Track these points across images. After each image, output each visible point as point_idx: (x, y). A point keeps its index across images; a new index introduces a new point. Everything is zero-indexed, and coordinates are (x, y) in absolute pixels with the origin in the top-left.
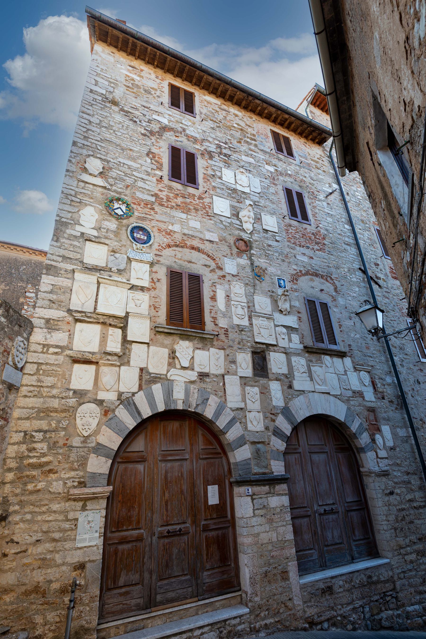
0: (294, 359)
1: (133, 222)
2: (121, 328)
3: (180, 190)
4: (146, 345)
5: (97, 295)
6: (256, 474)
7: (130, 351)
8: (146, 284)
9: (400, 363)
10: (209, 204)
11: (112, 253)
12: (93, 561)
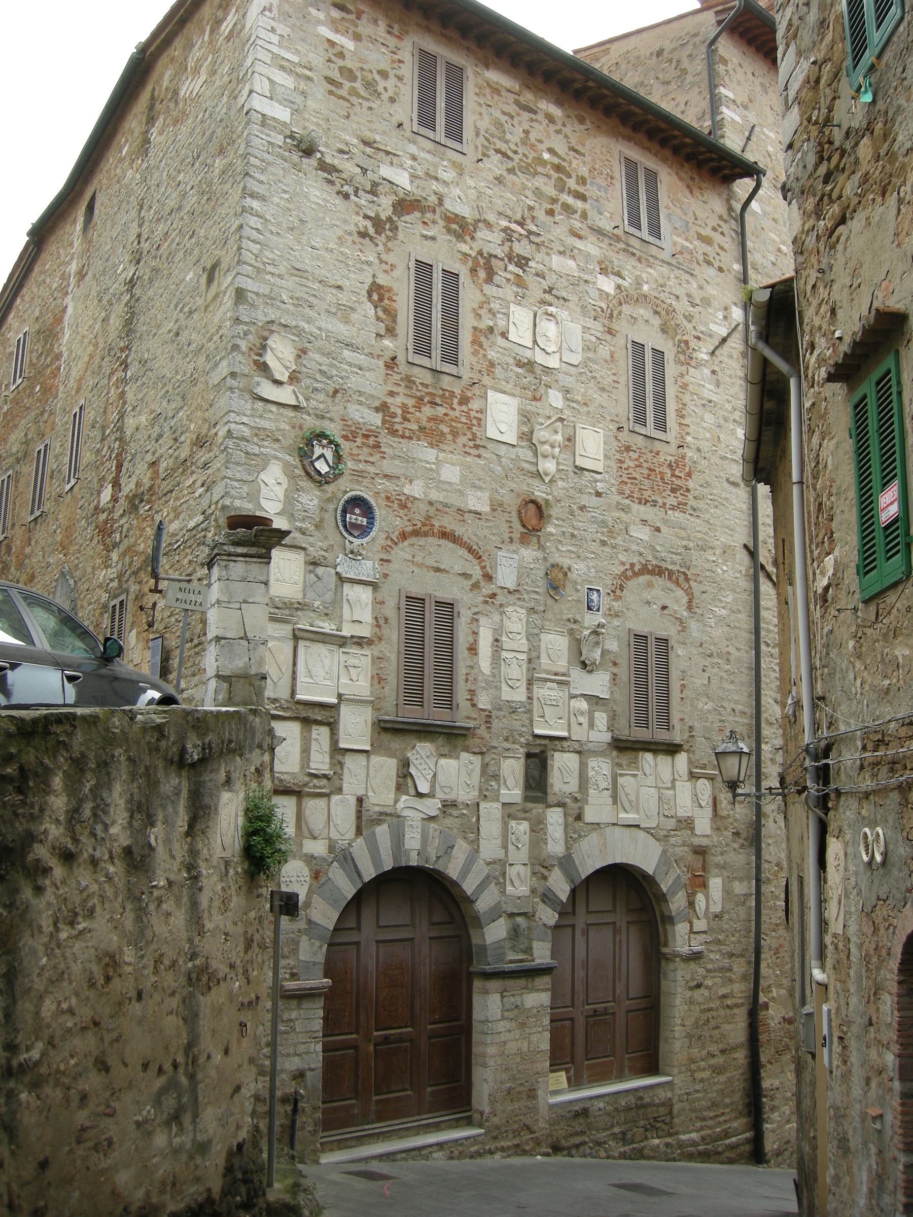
0: (593, 763)
1: (347, 488)
2: (329, 724)
3: (427, 386)
6: (511, 962)
7: (341, 764)
8: (365, 631)
9: (770, 756)
10: (479, 415)
11: (311, 567)
12: (313, 1070)
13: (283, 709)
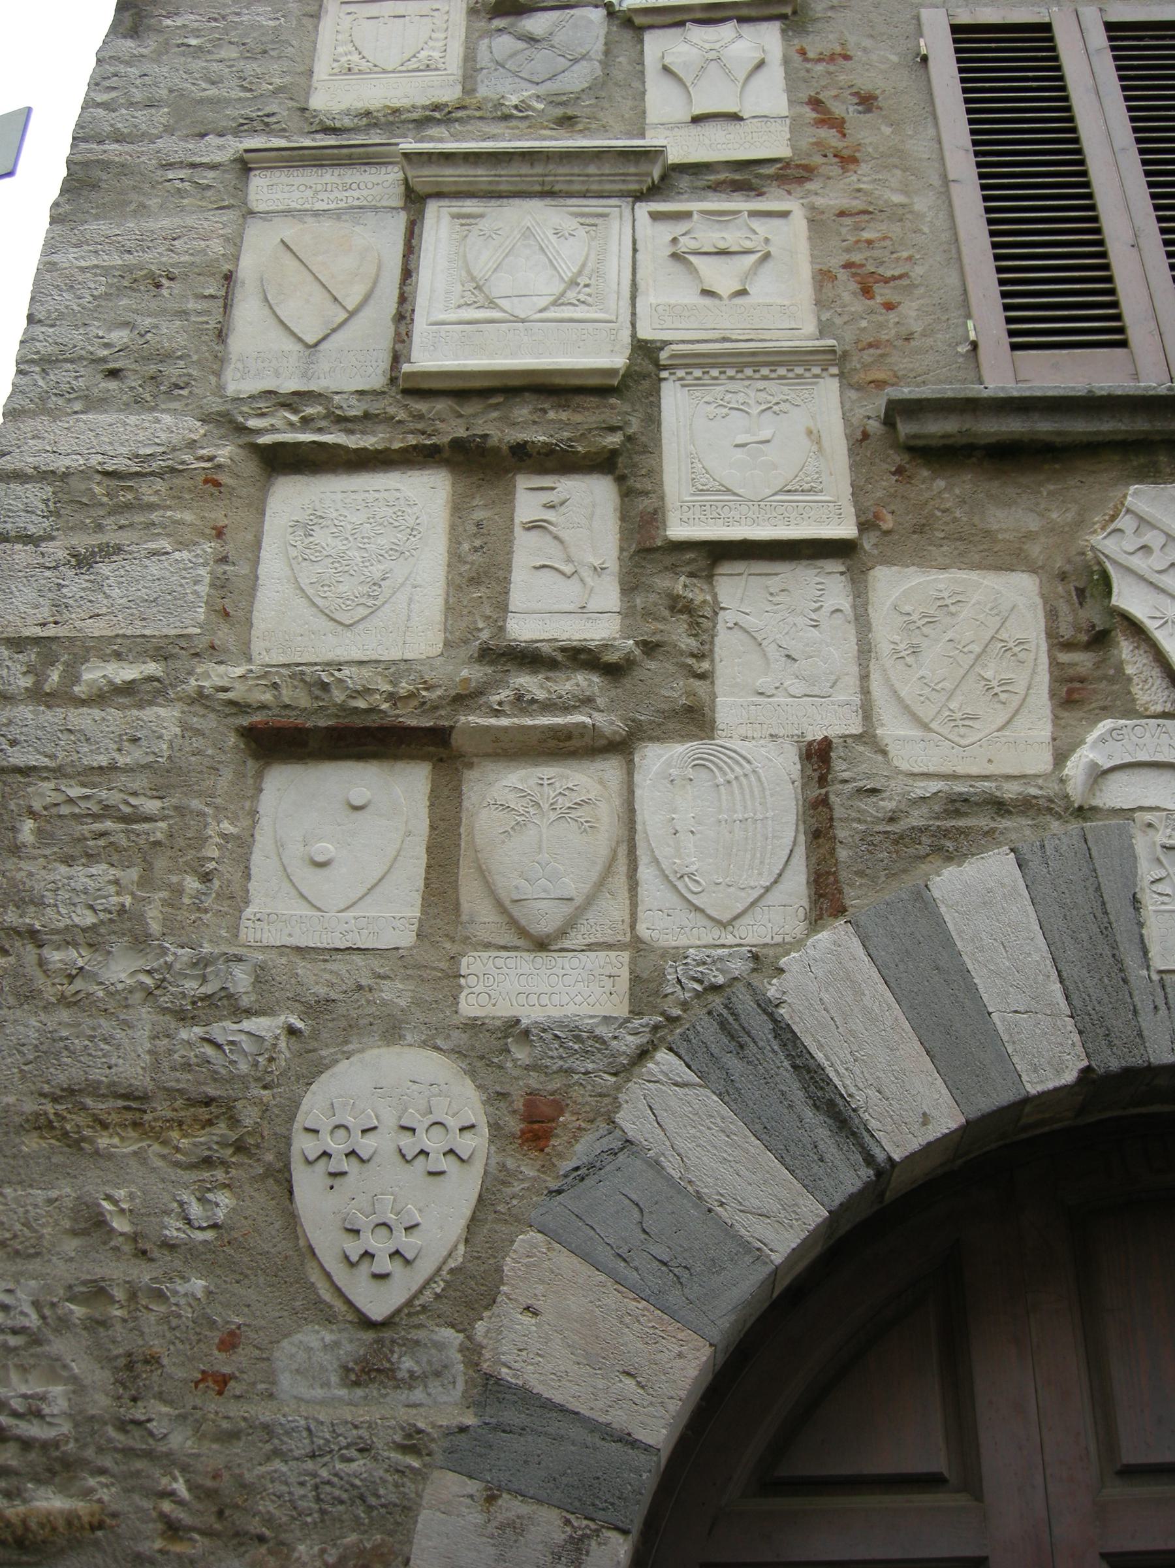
2: (602, 463)
4: (834, 566)
5: (407, 274)
11: (499, 23)
13: (342, 421)
